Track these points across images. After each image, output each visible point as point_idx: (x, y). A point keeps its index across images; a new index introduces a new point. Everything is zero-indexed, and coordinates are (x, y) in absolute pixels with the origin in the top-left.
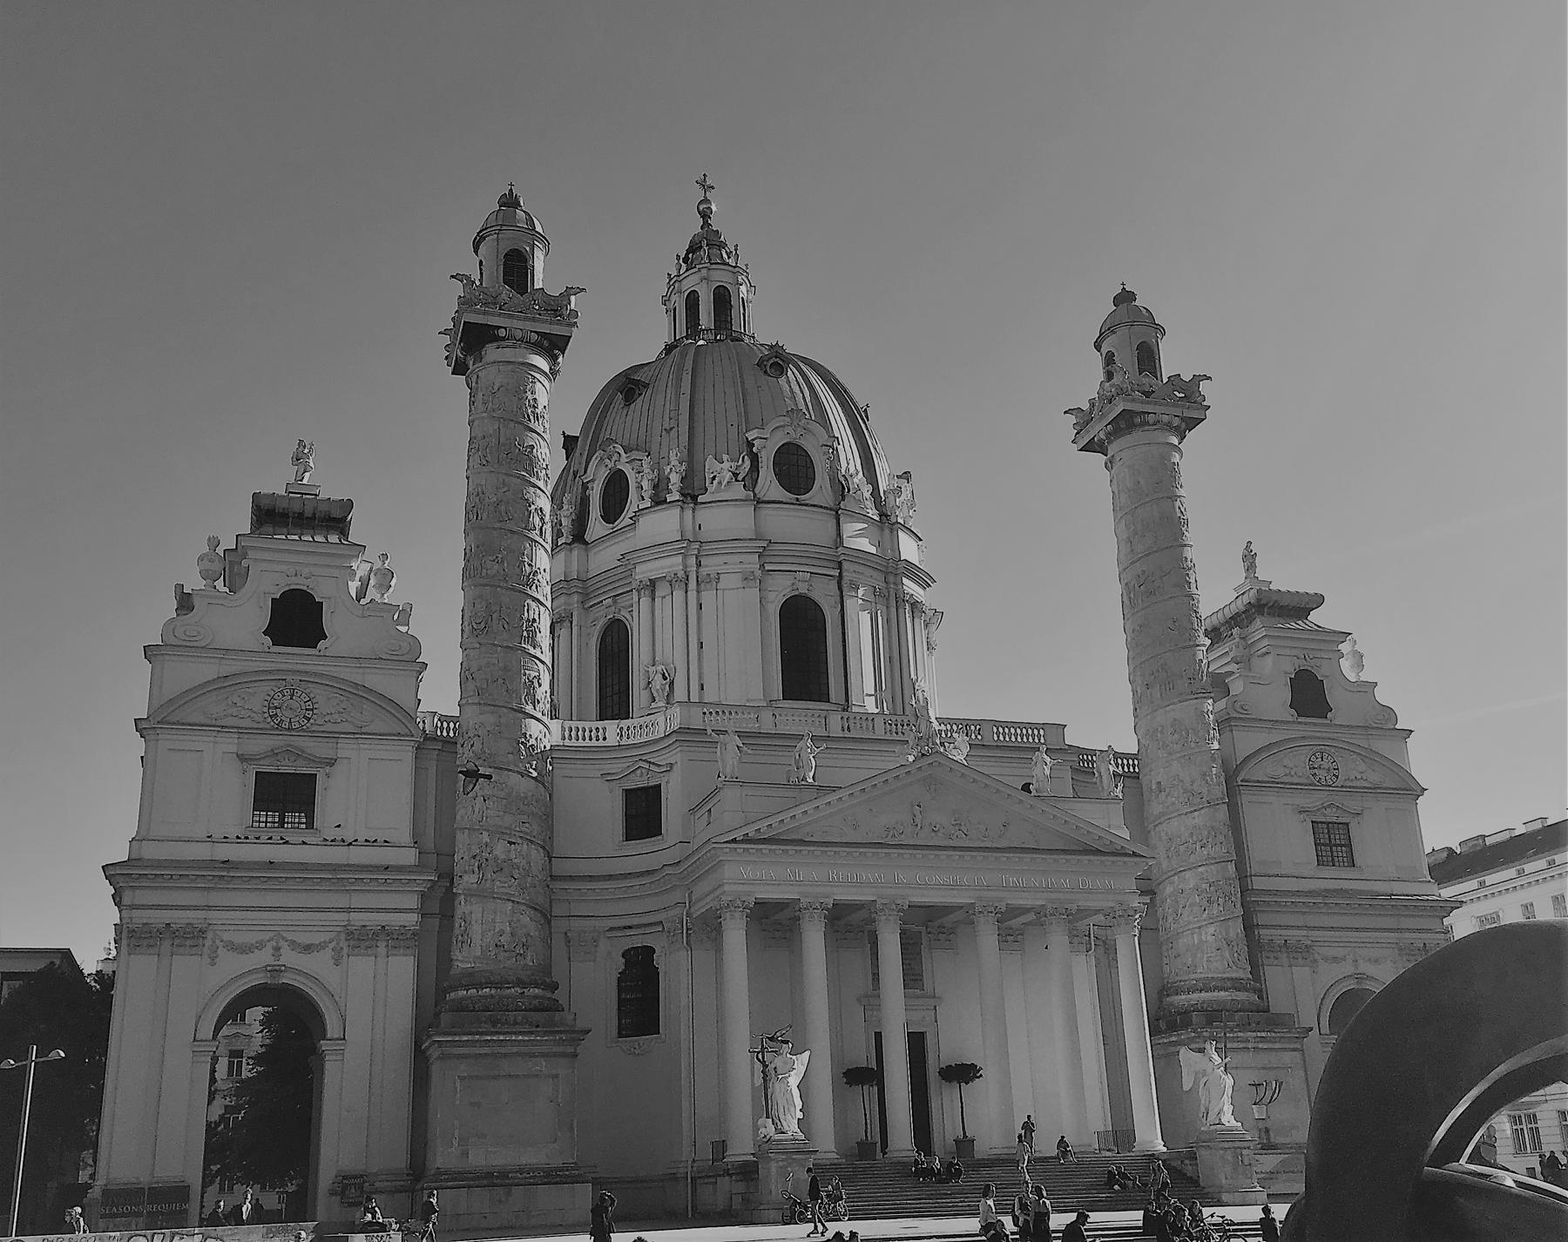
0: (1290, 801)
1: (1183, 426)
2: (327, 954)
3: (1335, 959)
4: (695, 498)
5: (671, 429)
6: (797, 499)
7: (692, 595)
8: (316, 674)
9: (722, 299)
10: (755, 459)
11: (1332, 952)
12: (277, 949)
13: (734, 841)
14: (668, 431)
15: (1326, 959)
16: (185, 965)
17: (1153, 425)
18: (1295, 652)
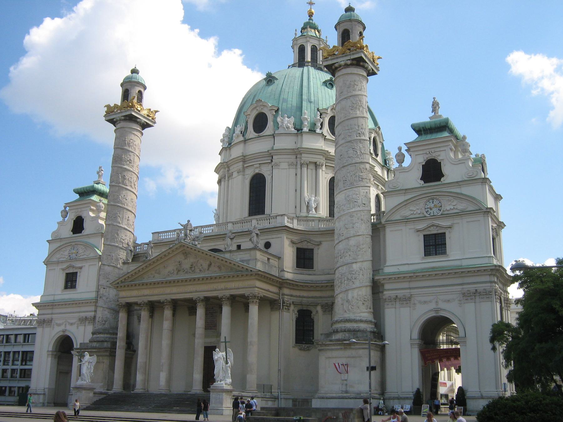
0: (412, 227)
1: (355, 62)
2: (76, 325)
3: (425, 302)
4: (231, 144)
6: (259, 135)
7: (226, 182)
8: (79, 242)
9: (302, 50)
10: (247, 122)
12: (66, 325)
13: (118, 283)
15: (420, 302)
16: (47, 330)
17: (340, 67)
18: (424, 152)
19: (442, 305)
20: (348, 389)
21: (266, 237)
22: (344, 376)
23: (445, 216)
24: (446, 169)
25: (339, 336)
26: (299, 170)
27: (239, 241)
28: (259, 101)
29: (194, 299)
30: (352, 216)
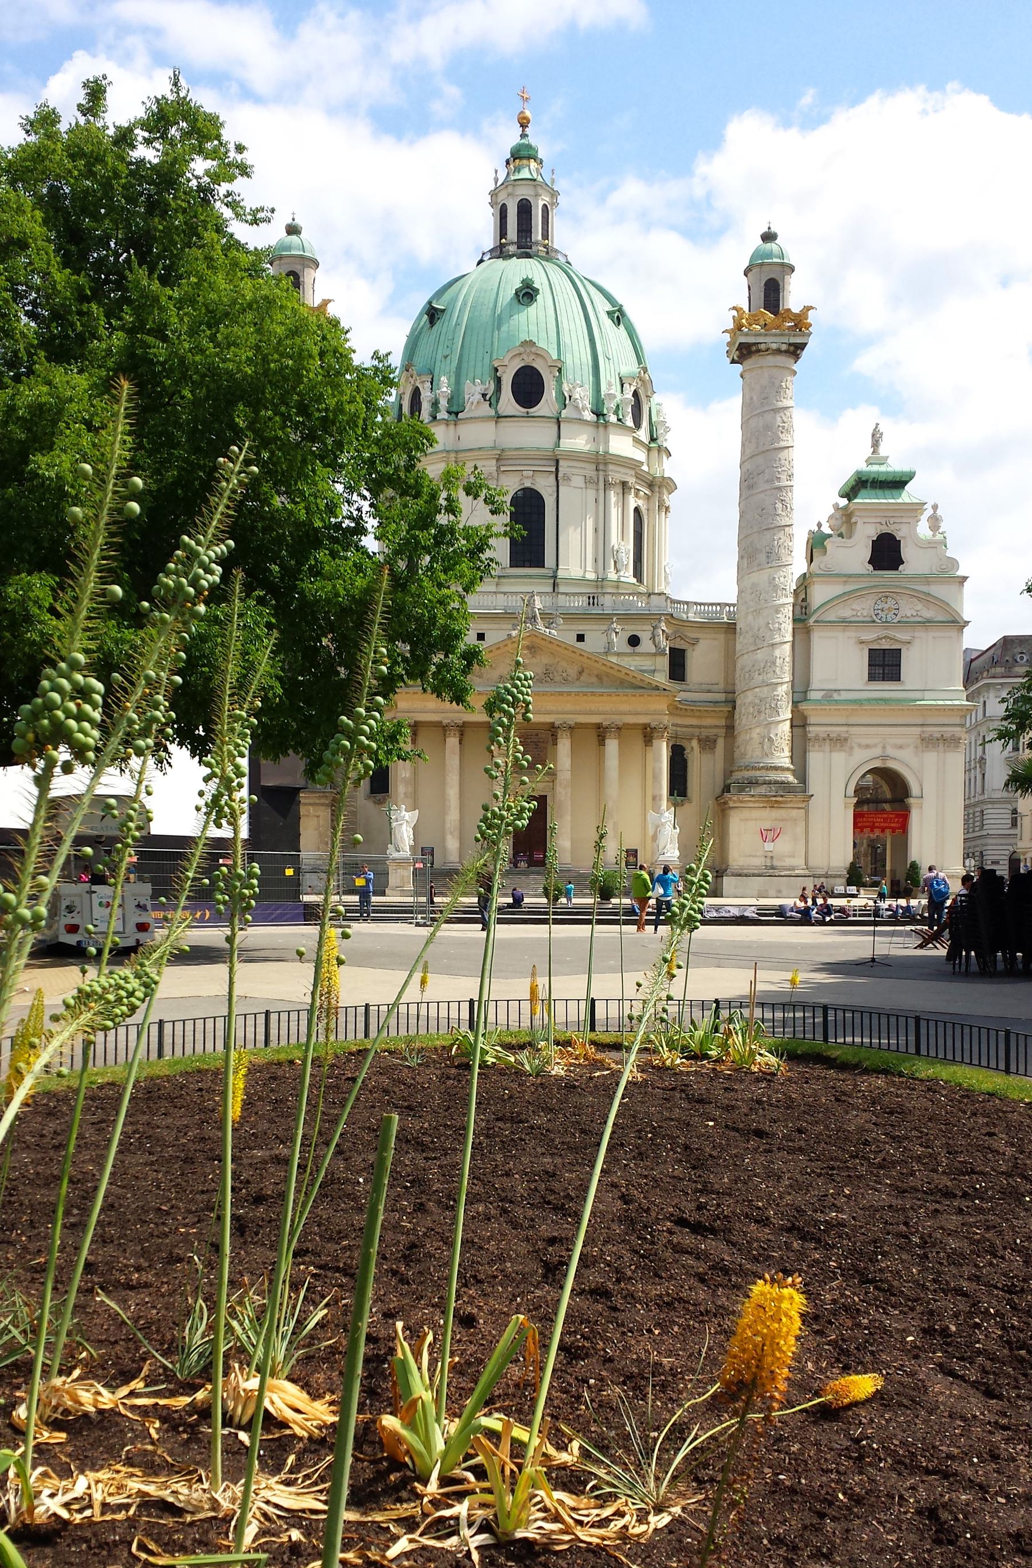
4: (457, 414)
5: (446, 357)
9: (525, 209)
10: (498, 381)
11: (864, 742)
14: (446, 357)
15: (860, 746)
19: (890, 751)
20: (776, 863)
21: (633, 627)
22: (769, 846)
23: (904, 624)
24: (906, 552)
25: (762, 790)
26: (602, 492)
27: (581, 627)
28: (531, 343)
29: (557, 723)
30: (778, 612)
